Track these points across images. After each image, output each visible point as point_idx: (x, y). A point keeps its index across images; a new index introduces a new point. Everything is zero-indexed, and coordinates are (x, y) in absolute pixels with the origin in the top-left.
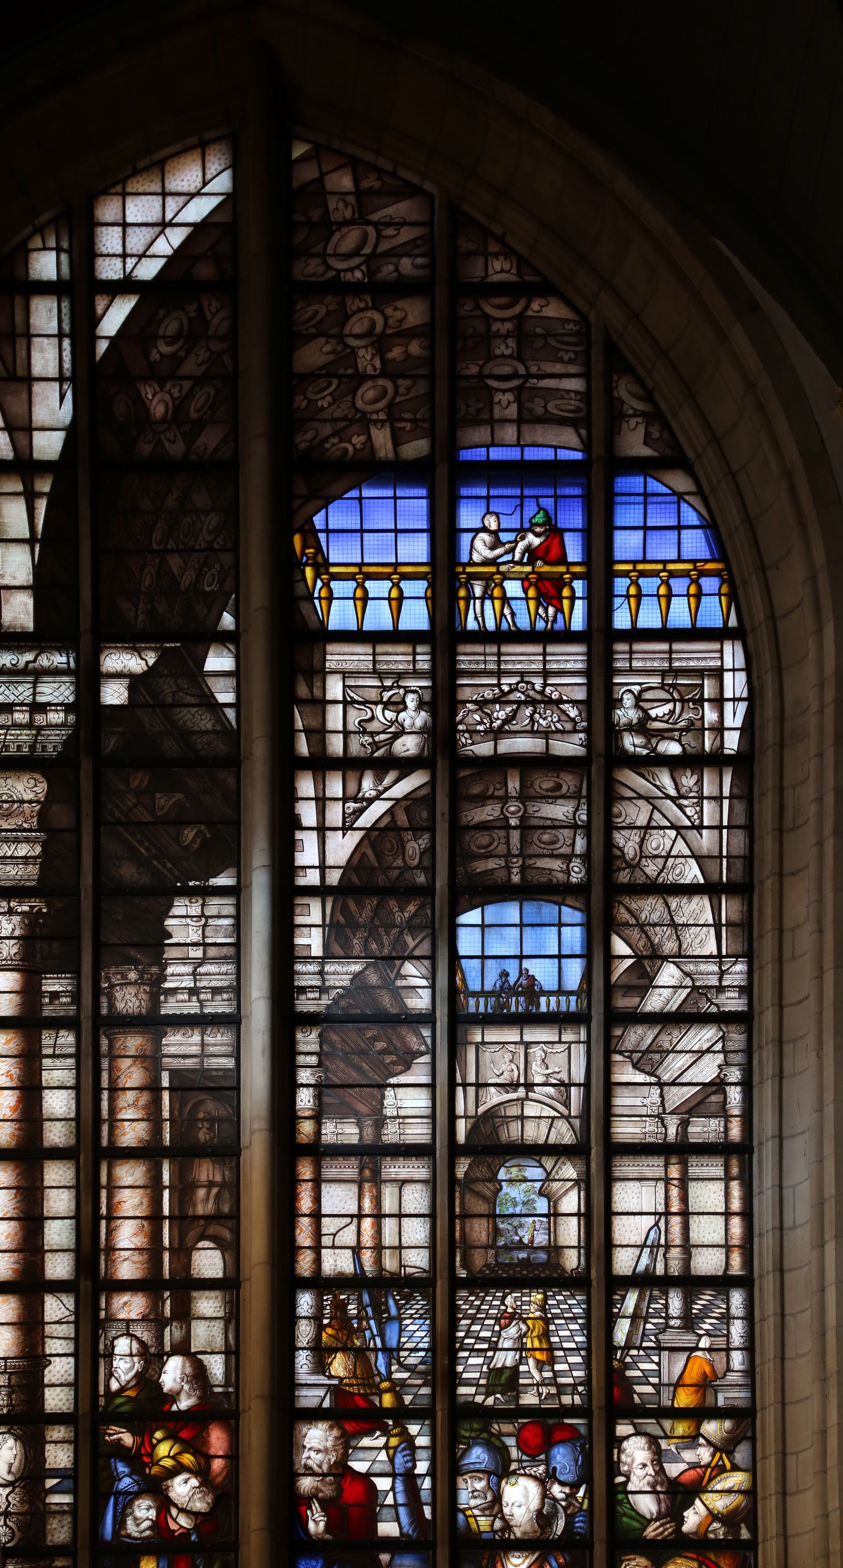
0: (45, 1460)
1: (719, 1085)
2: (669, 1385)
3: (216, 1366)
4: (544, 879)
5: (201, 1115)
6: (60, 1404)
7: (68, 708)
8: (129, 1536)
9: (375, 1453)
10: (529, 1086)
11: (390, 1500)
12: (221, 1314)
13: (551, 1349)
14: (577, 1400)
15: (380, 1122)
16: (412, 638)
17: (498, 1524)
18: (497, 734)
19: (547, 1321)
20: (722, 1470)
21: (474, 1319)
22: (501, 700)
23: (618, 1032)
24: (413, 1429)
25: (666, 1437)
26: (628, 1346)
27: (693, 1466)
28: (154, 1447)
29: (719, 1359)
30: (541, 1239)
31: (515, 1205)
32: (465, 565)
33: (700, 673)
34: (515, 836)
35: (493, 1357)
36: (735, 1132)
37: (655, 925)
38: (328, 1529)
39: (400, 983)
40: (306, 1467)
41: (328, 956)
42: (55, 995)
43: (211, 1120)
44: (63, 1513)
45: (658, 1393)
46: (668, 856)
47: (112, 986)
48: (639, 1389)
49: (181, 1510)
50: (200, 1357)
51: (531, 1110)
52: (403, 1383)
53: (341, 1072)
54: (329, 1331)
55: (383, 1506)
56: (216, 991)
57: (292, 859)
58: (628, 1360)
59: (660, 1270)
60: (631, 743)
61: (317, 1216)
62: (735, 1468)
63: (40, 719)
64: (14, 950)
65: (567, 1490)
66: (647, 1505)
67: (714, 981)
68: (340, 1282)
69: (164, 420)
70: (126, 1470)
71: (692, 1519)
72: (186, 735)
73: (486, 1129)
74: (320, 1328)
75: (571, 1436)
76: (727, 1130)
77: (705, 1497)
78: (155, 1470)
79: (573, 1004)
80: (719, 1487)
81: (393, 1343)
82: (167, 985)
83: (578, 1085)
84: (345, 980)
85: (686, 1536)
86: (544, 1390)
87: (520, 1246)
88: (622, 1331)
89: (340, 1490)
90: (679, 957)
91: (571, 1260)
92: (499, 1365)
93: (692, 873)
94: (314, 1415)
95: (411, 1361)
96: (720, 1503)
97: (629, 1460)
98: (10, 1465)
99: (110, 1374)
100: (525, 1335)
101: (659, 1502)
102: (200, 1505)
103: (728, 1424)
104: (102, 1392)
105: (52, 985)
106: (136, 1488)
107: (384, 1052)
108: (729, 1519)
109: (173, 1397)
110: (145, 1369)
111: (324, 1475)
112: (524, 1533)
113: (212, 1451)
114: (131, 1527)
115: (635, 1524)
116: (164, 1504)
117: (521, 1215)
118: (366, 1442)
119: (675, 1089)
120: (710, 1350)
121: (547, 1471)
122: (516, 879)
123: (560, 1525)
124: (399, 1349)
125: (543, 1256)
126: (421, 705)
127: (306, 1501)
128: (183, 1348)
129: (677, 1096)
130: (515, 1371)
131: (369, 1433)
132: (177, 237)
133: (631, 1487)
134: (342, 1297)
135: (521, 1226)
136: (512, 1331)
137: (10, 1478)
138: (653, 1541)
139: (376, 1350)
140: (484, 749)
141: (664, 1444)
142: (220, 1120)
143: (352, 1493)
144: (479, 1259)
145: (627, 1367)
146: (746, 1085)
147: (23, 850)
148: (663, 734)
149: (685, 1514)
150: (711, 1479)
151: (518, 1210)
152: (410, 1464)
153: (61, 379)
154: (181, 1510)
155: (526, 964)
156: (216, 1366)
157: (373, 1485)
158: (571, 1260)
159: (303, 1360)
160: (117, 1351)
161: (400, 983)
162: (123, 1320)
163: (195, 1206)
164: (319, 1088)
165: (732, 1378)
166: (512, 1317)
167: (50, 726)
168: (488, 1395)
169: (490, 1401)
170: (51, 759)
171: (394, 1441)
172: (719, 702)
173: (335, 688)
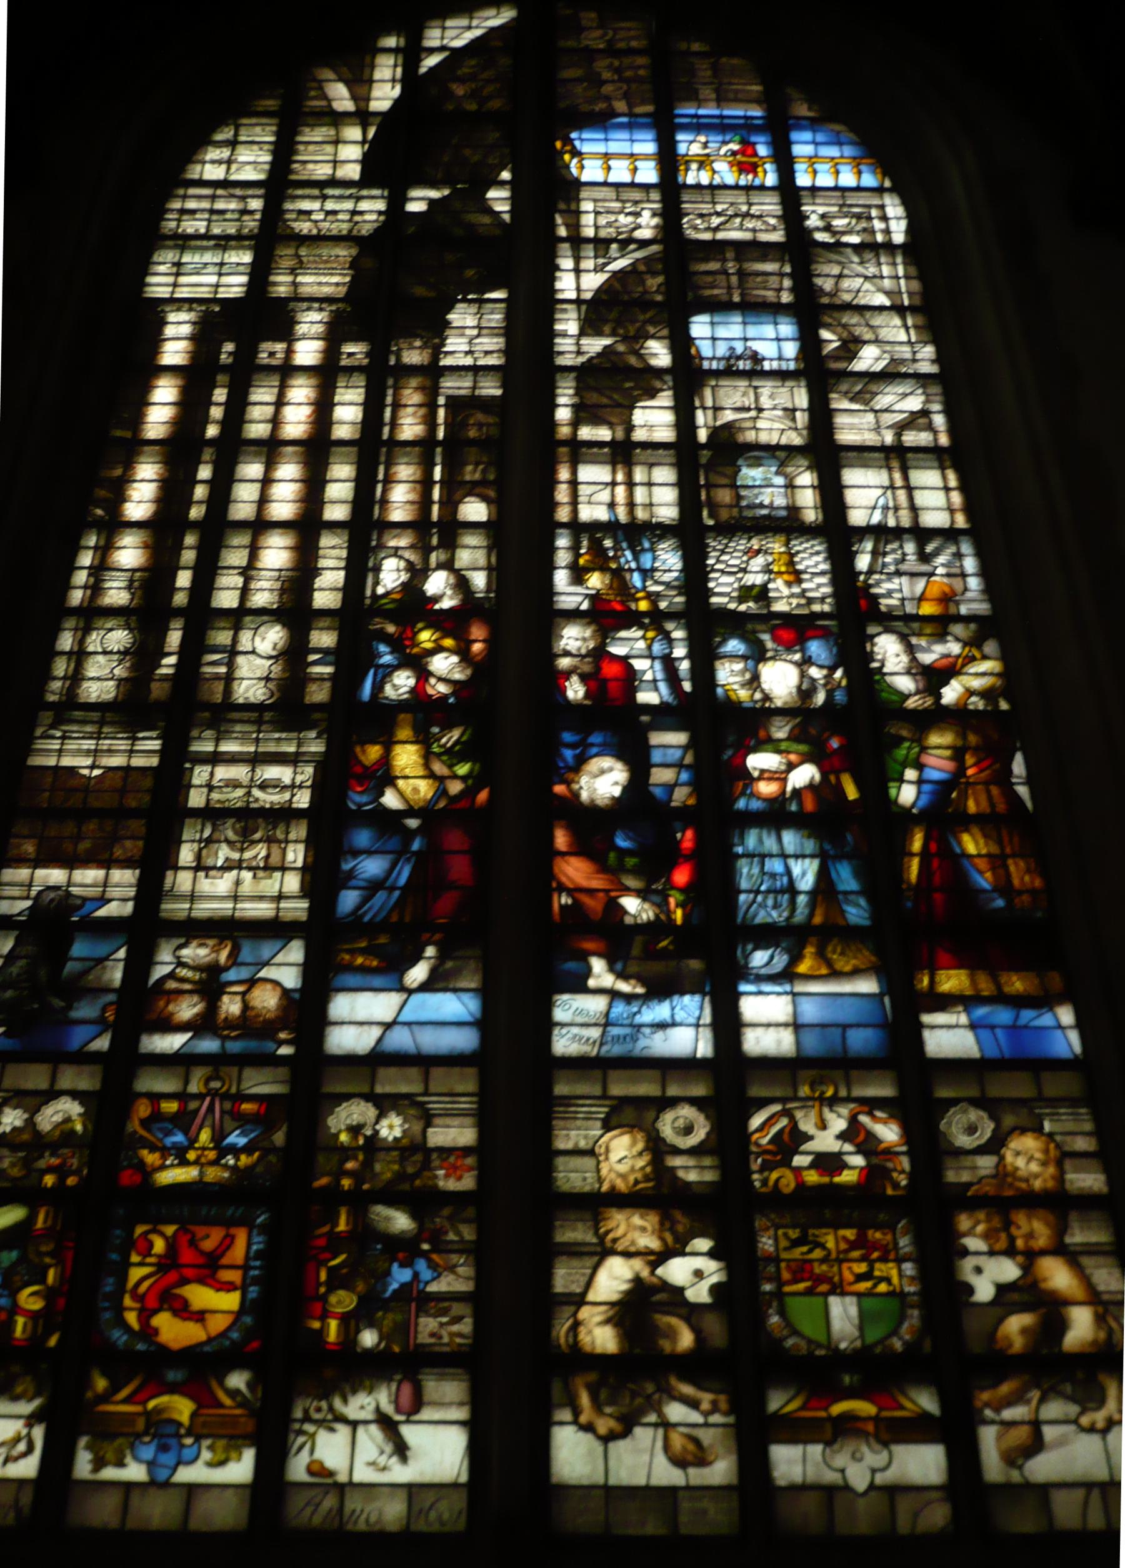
0: (308, 642)
1: (925, 413)
2: (912, 599)
3: (479, 580)
4: (760, 300)
5: (471, 422)
6: (327, 603)
7: (380, 213)
8: (387, 698)
9: (632, 642)
10: (760, 410)
11: (648, 676)
12: (485, 544)
13: (798, 573)
14: (826, 608)
15: (630, 428)
16: (646, 187)
17: (758, 696)
18: (716, 229)
19: (792, 556)
20: (973, 659)
21: (723, 552)
22: (718, 214)
23: (832, 381)
24: (669, 626)
25: (914, 634)
26: (871, 572)
27: (946, 656)
28: (416, 634)
29: (957, 584)
30: (780, 501)
31: (755, 480)
32: (684, 156)
33: (869, 207)
34: (734, 280)
35: (741, 579)
36: (944, 440)
37: (854, 326)
38: (587, 695)
39: (643, 351)
40: (564, 650)
41: (582, 333)
42: (350, 355)
43: (480, 425)
44: (323, 680)
45: (903, 604)
46: (858, 291)
47: (400, 350)
48: (883, 601)
49: (440, 679)
50: (463, 572)
51: (760, 424)
52: (658, 594)
53: (593, 398)
54: (587, 557)
55: (641, 681)
56: (487, 353)
57: (553, 286)
58: (871, 582)
59: (891, 523)
60: (820, 237)
61: (574, 483)
62: (985, 657)
63: (357, 218)
64: (321, 330)
65: (825, 672)
66: (905, 684)
67: (909, 356)
68: (595, 528)
69: (464, 96)
70: (387, 650)
71: (951, 693)
72: (471, 226)
73: (725, 435)
74: (578, 556)
75: (824, 634)
76: (936, 440)
77: (961, 678)
78: (415, 650)
79: (792, 366)
80: (972, 671)
81: (648, 566)
82: (445, 349)
83: (803, 410)
84: (598, 349)
85: (946, 708)
86: (795, 602)
87: (761, 506)
88: (863, 562)
89: (598, 668)
90: (877, 341)
91: (811, 516)
92: (749, 583)
93: (881, 300)
94: (574, 615)
95: (667, 577)
96: (976, 683)
97: (882, 651)
98: (276, 644)
99: (377, 583)
100: (772, 563)
101: (916, 681)
102: (458, 676)
103: (973, 626)
104: (368, 593)
105: (349, 348)
106: (396, 663)
107: (631, 388)
108: (986, 694)
109: (436, 599)
110: (411, 580)
111: (583, 657)
112: (786, 703)
113: (473, 637)
114: (389, 691)
115: (894, 698)
116: (423, 674)
117: (760, 486)
118: (623, 634)
119: (886, 415)
120: (948, 575)
121: (803, 657)
122: (736, 299)
123: (820, 698)
124: (654, 570)
125: (783, 513)
126: (654, 215)
127: (567, 674)
128: (448, 565)
129: (889, 419)
130: (764, 589)
131: (628, 627)
132: (478, 33)
133: (885, 670)
134: (598, 535)
135: (760, 493)
136: (759, 562)
137: (274, 653)
138: (914, 711)
139: (631, 570)
140: (707, 236)
141: (914, 640)
142: (489, 425)
143: (610, 670)
144: (724, 515)
145: (871, 586)
146: (948, 412)
147: (335, 279)
148: (844, 233)
149: (943, 691)
150: (964, 665)
151: (757, 483)
152: (667, 651)
153: (394, 80)
154: (440, 679)
155: (749, 344)
156: (479, 580)
157: (631, 666)
158: (811, 516)
159: (561, 578)
160: (384, 567)
161: (643, 351)
162: (392, 547)
163: (463, 475)
164: (577, 408)
165: (969, 595)
166: (758, 552)
167: (365, 221)
168: (740, 603)
169: (743, 608)
170: (363, 237)
171: (650, 634)
172: (884, 218)
173: (587, 206)
